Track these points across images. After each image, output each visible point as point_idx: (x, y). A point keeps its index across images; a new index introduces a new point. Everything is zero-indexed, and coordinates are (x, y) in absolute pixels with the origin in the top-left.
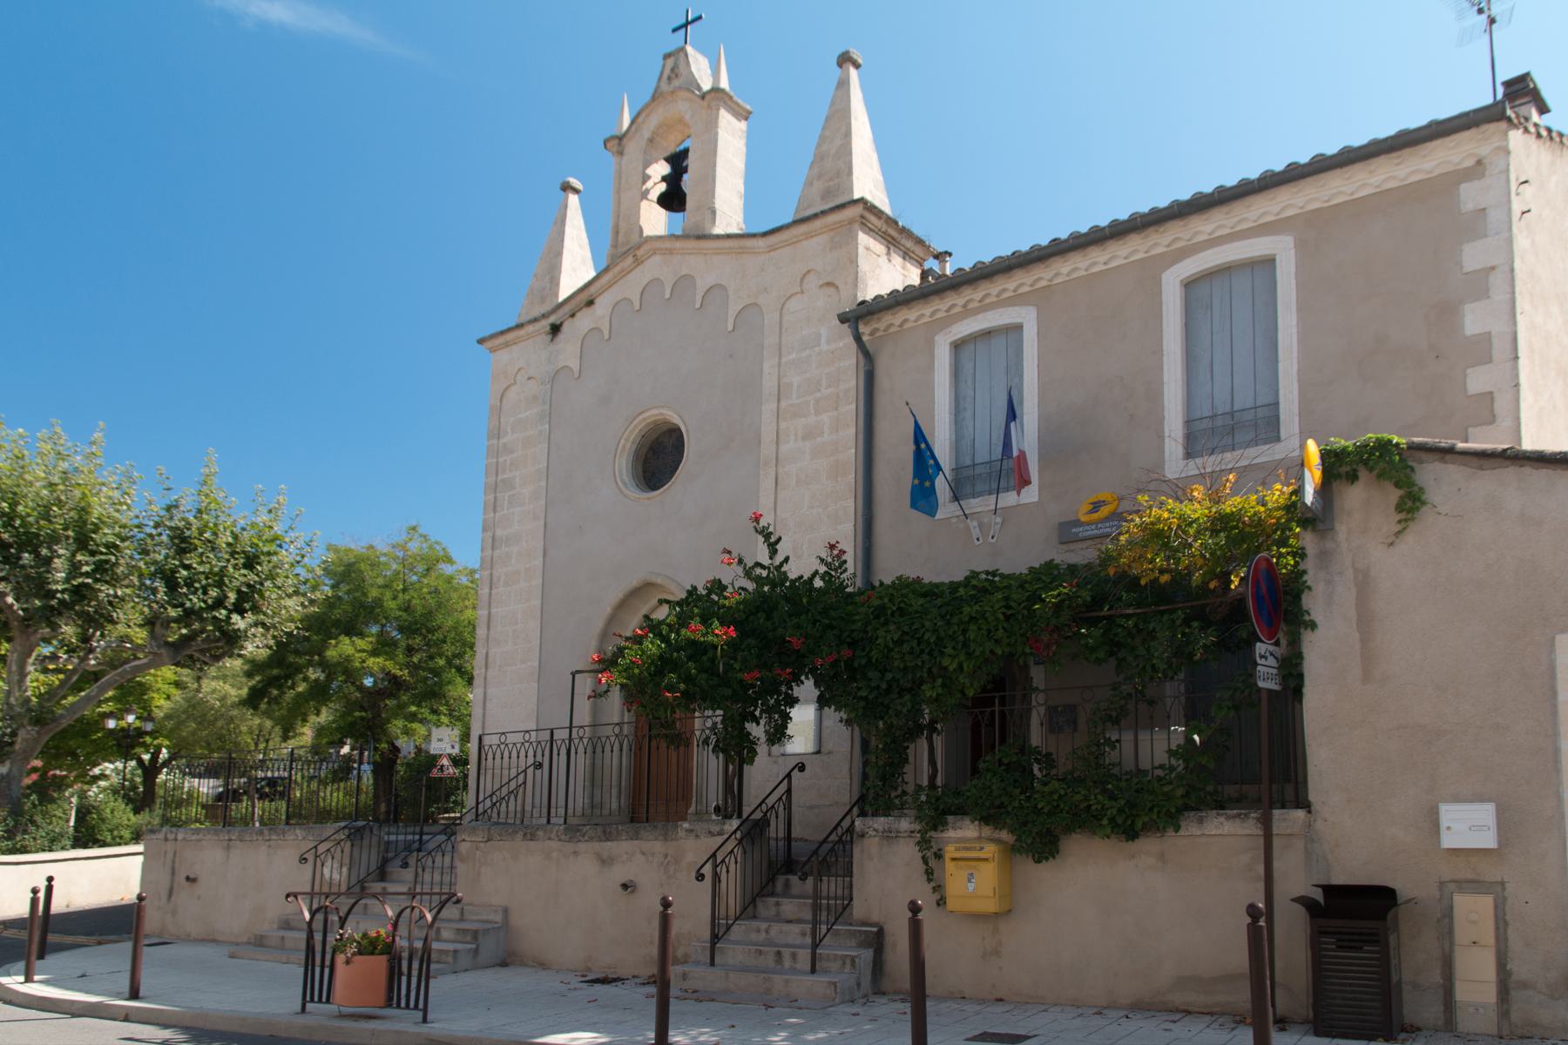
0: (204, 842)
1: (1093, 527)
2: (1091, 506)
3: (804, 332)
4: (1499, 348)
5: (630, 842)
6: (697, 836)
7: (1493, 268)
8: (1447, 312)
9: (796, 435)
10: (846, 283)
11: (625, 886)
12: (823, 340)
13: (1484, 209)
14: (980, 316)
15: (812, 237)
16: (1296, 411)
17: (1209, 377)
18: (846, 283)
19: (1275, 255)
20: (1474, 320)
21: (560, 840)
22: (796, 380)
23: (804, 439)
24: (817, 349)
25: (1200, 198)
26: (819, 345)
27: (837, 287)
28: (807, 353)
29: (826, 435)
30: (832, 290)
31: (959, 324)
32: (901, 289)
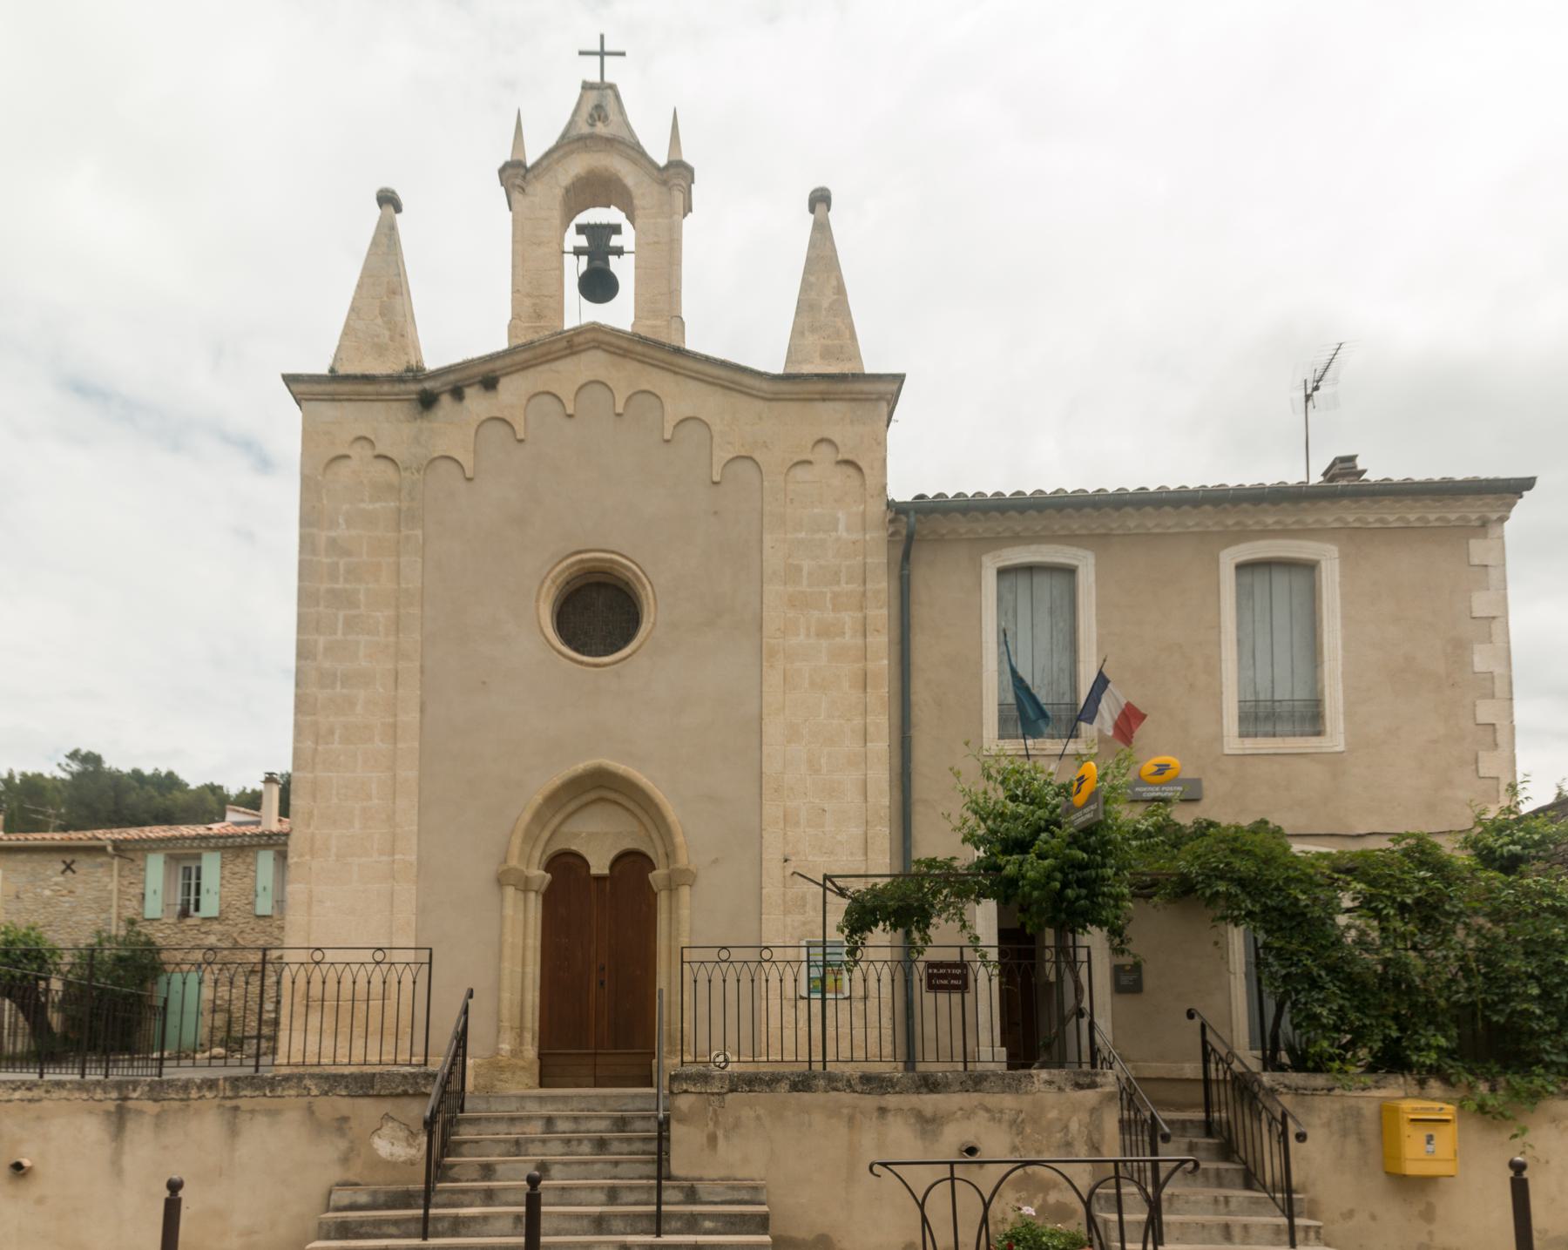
0: (45, 1103)
1: (1157, 789)
2: (1157, 768)
3: (816, 510)
4: (1499, 686)
5: (966, 1095)
6: (1060, 1089)
7: (1494, 618)
8: (1459, 649)
9: (808, 629)
10: (872, 468)
11: (18, 1166)
12: (841, 526)
13: (1486, 566)
14: (1033, 547)
15: (829, 400)
16: (1341, 709)
17: (1251, 662)
18: (872, 468)
19: (1077, 567)
20: (1482, 660)
21: (854, 1091)
22: (807, 565)
23: (818, 635)
24: (833, 534)
25: (1448, 482)
26: (837, 531)
27: (859, 469)
28: (821, 535)
29: (847, 636)
30: (851, 471)
31: (1010, 549)
32: (1028, 493)
